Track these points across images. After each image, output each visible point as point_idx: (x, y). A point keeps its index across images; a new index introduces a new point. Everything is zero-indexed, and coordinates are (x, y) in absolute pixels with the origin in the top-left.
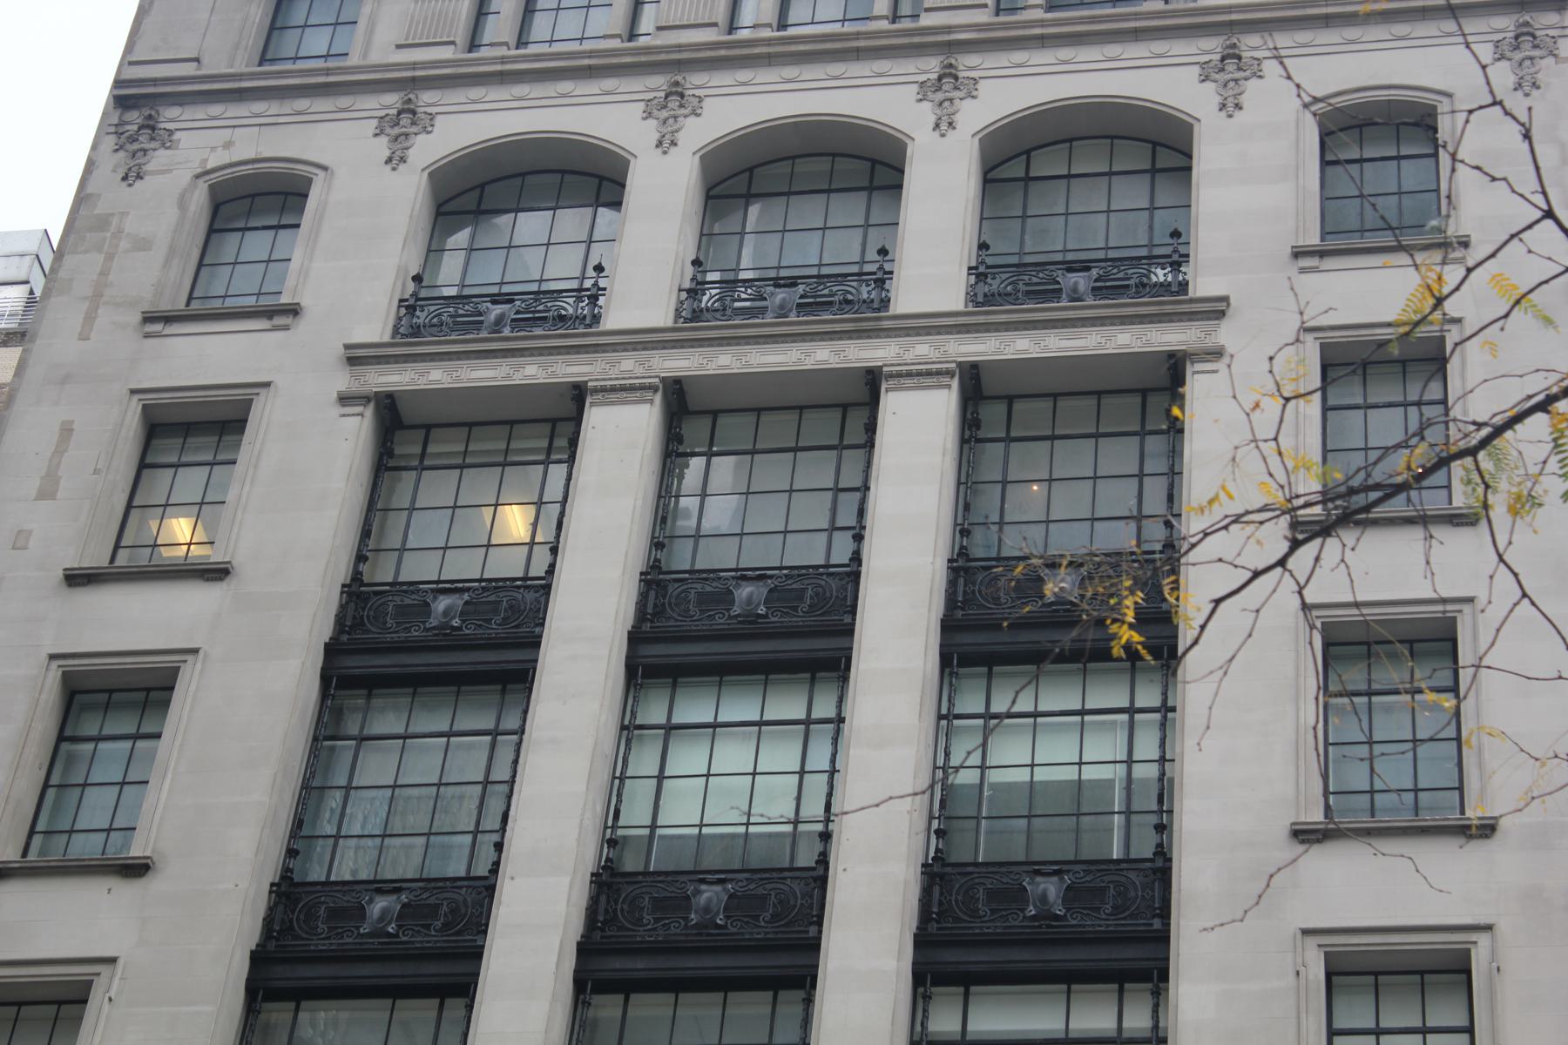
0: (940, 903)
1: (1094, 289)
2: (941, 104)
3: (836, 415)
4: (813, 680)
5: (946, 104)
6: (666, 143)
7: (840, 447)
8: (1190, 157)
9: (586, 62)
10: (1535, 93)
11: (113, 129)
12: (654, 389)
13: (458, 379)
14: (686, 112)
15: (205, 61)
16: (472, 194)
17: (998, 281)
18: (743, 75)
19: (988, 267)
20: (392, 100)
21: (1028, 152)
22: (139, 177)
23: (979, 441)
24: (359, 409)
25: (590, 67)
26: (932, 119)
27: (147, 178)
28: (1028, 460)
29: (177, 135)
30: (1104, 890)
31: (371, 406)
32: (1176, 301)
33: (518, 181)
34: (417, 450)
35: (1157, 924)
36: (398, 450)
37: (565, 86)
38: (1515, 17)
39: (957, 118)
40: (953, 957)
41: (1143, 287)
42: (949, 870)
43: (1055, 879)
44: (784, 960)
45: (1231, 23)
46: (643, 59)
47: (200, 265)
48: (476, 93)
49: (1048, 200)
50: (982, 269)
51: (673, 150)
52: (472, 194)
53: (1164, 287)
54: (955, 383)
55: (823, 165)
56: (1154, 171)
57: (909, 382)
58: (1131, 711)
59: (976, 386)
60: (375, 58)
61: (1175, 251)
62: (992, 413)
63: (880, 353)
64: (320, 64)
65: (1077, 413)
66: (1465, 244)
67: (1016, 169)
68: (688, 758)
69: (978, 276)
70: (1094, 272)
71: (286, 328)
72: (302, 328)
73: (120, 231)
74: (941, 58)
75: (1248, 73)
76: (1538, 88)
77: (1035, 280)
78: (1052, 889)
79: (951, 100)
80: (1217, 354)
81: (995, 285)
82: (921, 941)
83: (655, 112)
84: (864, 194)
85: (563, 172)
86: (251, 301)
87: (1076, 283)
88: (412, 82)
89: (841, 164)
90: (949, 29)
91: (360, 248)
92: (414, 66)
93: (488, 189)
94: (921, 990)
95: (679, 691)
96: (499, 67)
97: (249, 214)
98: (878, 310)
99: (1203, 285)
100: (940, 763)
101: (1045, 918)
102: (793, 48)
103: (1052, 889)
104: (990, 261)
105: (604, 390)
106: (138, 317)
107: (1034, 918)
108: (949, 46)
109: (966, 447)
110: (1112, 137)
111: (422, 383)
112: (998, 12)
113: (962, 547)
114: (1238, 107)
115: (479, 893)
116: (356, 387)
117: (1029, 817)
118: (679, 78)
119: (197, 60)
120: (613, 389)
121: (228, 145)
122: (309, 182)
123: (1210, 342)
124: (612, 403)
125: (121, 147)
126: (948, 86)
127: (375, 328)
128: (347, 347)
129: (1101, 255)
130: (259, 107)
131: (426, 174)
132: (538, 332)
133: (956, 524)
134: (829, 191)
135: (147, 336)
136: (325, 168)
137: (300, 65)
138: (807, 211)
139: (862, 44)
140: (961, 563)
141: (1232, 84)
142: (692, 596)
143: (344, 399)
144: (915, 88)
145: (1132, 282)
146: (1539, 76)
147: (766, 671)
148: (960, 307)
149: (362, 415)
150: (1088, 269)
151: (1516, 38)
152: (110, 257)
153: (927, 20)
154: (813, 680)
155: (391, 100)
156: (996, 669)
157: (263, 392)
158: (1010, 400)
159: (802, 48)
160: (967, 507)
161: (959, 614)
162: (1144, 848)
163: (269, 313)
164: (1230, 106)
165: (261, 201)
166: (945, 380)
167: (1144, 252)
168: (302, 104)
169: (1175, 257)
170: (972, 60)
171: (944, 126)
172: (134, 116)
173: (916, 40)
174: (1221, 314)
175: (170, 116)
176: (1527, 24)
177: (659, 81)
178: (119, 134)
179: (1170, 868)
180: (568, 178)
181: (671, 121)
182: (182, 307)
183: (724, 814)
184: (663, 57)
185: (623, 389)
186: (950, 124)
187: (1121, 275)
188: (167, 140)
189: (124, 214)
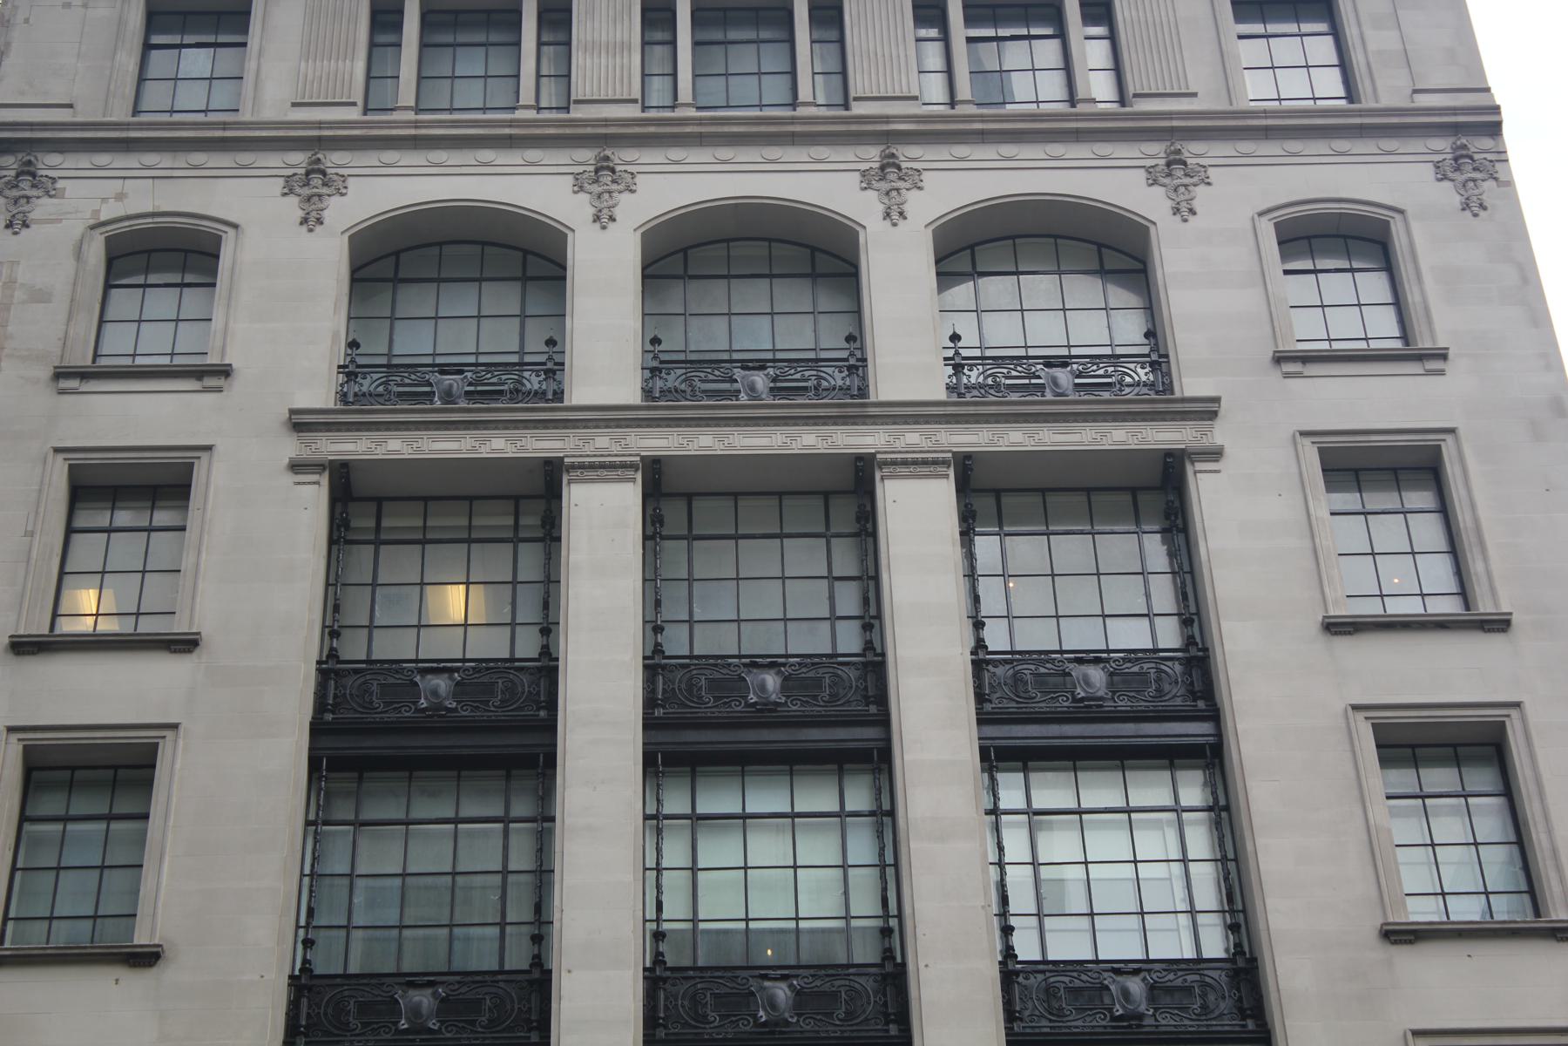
1: (772, 389)
2: (887, 194)
3: (818, 502)
4: (508, 777)
6: (603, 218)
7: (516, 540)
8: (565, 269)
9: (507, 131)
10: (1482, 213)
14: (621, 187)
15: (79, 107)
16: (391, 261)
18: (676, 154)
19: (662, 362)
20: (299, 159)
21: (972, 247)
22: (25, 225)
24: (315, 478)
25: (510, 137)
27: (33, 227)
28: (713, 559)
29: (60, 184)
31: (326, 475)
32: (1161, 400)
33: (436, 250)
34: (372, 523)
36: (353, 524)
37: (487, 155)
38: (1452, 139)
39: (906, 207)
41: (517, 393)
42: (315, 982)
43: (429, 991)
45: (1172, 130)
46: (568, 131)
47: (102, 321)
48: (390, 156)
49: (416, 300)
50: (351, 368)
51: (318, 229)
52: (391, 261)
53: (540, 395)
54: (639, 476)
57: (904, 470)
58: (841, 814)
59: (661, 485)
60: (269, 114)
61: (550, 359)
62: (674, 514)
63: (869, 440)
64: (200, 117)
65: (759, 515)
67: (963, 263)
68: (718, 850)
69: (348, 374)
70: (771, 371)
71: (219, 390)
72: (238, 387)
74: (882, 147)
75: (1195, 180)
76: (1485, 209)
77: (1014, 373)
78: (782, 992)
80: (1216, 454)
81: (366, 385)
83: (298, 190)
84: (519, 284)
85: (484, 244)
86: (166, 360)
87: (451, 386)
88: (318, 142)
90: (887, 119)
91: (285, 311)
92: (320, 125)
93: (403, 256)
95: (700, 782)
96: (413, 132)
97: (147, 270)
98: (1164, 392)
99: (1191, 385)
100: (651, 863)
101: (418, 1032)
102: (726, 129)
103: (424, 999)
104: (361, 361)
105: (582, 466)
106: (45, 373)
107: (406, 1031)
108: (886, 136)
109: (335, 548)
110: (1013, 238)
111: (380, 453)
112: (366, 111)
113: (332, 649)
114: (1192, 212)
116: (306, 454)
117: (451, 926)
118: (608, 152)
119: (70, 106)
120: (592, 466)
121: (120, 197)
122: (217, 240)
124: (592, 481)
126: (604, 180)
127: (319, 394)
128: (293, 412)
129: (472, 359)
130: (150, 159)
131: (346, 237)
132: (1106, 395)
133: (324, 627)
134: (480, 280)
135: (62, 392)
136: (235, 226)
137: (177, 117)
138: (460, 300)
139: (798, 128)
140: (330, 665)
141: (1182, 189)
142: (374, 688)
143: (296, 467)
144: (281, 181)
145: (505, 387)
146: (1484, 197)
147: (792, 762)
148: (331, 405)
149: (317, 483)
150: (763, 368)
153: (858, 109)
154: (508, 777)
156: (514, 772)
157: (204, 455)
158: (689, 497)
159: (735, 129)
160: (336, 608)
161: (329, 717)
162: (518, 958)
163: (199, 373)
164: (1184, 210)
166: (941, 469)
167: (514, 359)
168: (198, 158)
169: (550, 365)
170: (914, 151)
171: (895, 216)
173: (854, 128)
174: (1213, 415)
175: (49, 162)
176: (1464, 147)
177: (587, 155)
179: (550, 980)
180: (447, 249)
181: (606, 196)
182: (89, 363)
183: (769, 907)
184: (589, 130)
185: (603, 466)
187: (798, 376)
188: (48, 188)
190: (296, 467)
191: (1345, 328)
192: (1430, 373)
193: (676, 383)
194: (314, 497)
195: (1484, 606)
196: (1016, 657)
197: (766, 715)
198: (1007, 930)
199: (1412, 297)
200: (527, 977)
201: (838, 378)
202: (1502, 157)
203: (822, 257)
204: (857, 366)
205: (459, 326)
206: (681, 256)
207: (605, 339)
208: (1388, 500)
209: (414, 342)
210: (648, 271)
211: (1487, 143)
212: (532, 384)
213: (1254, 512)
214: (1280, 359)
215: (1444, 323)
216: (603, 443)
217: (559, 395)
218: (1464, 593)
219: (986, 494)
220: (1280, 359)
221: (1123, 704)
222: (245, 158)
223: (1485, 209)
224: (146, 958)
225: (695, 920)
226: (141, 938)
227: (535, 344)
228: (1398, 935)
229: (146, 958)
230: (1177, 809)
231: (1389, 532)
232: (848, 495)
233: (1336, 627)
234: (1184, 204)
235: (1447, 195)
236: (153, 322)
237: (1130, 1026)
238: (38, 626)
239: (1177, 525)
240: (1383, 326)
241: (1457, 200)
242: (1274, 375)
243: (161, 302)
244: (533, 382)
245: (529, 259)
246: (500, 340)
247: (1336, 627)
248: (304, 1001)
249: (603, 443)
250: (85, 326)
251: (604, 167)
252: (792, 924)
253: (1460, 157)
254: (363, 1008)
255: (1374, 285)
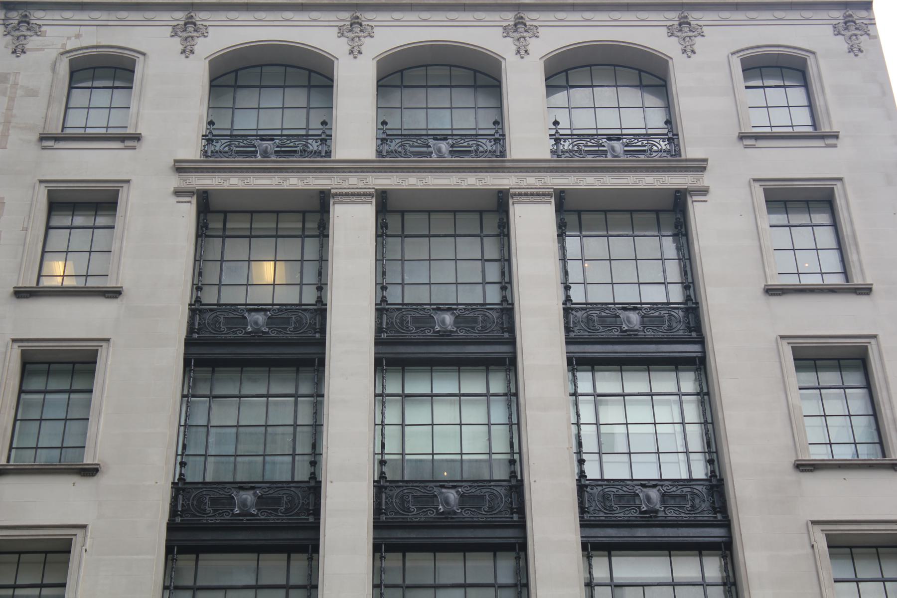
0: (386, 503)
1: (450, 151)
2: (518, 40)
3: (477, 217)
4: (298, 371)
5: (522, 40)
7: (303, 236)
8: (333, 81)
10: (860, 54)
11: (1, 22)
12: (370, 195)
13: (307, 184)
14: (365, 34)
16: (233, 75)
17: (219, 144)
19: (388, 135)
20: (181, 15)
22: (23, 52)
23: (207, 236)
26: (514, 48)
27: (28, 53)
28: (415, 249)
29: (43, 28)
30: (280, 499)
31: (195, 197)
32: (674, 160)
33: (259, 69)
34: (220, 225)
35: (311, 519)
36: (210, 226)
37: (288, 15)
39: (529, 48)
40: (399, 535)
41: (304, 152)
42: (186, 486)
43: (251, 492)
44: (301, 535)
47: (67, 108)
48: (233, 15)
49: (247, 98)
50: (210, 136)
51: (191, 56)
52: (233, 75)
53: (318, 153)
54: (374, 200)
55: (445, 71)
56: (310, 87)
58: (488, 395)
59: (386, 205)
61: (324, 132)
62: (394, 222)
63: (506, 181)
65: (442, 224)
66: (836, 137)
68: (417, 414)
69: (208, 140)
70: (450, 141)
71: (134, 148)
72: (144, 147)
73: (15, 84)
75: (695, 33)
76: (862, 52)
77: (589, 144)
78: (452, 495)
79: (524, 38)
80: (704, 191)
81: (218, 146)
82: (172, 528)
85: (286, 66)
86: (103, 131)
87: (267, 147)
89: (455, 71)
91: (172, 102)
93: (240, 73)
94: (170, 556)
95: (407, 375)
97: (93, 79)
98: (675, 155)
99: (691, 151)
100: (378, 421)
101: (245, 515)
103: (249, 497)
104: (215, 132)
105: (341, 194)
106: (37, 136)
107: (238, 515)
109: (200, 239)
110: (590, 66)
111: (226, 185)
113: (197, 297)
114: (693, 52)
115: (313, 489)
116: (183, 185)
117: (264, 456)
118: (358, 14)
120: (347, 195)
121: (78, 36)
122: (133, 62)
123: (699, 184)
125: (9, 33)
127: (192, 151)
128: (176, 161)
129: (279, 132)
130: (96, 14)
132: (642, 157)
133: (193, 284)
134: (284, 87)
135: (44, 148)
136: (144, 54)
138: (272, 98)
140: (197, 306)
141: (688, 39)
142: (222, 320)
143: (178, 193)
144: (170, 29)
145: (298, 149)
146: (861, 45)
147: (460, 365)
148: (198, 158)
150: (446, 139)
151: (846, 23)
152: (12, 99)
154: (298, 371)
155: (180, 16)
156: (301, 369)
157: (125, 185)
160: (200, 274)
161: (196, 336)
162: (303, 474)
163: (122, 138)
164: (688, 51)
165: (107, 71)
166: (547, 199)
167: (303, 132)
168: (123, 14)
169: (323, 136)
170: (534, 15)
171: (523, 52)
172: (15, 15)
174: (703, 169)
176: (851, 16)
177: (346, 15)
178: (6, 26)
180: (265, 69)
181: (357, 39)
182: (60, 131)
183: (446, 446)
185: (353, 194)
186: (526, 51)
187: (466, 144)
188: (36, 30)
189: (17, 74)
190: (178, 193)
191: (780, 119)
192: (828, 146)
193: (397, 147)
194: (188, 210)
195: (857, 280)
196: (588, 306)
197: (445, 338)
198: (581, 462)
199: (819, 102)
200: (307, 485)
201: (488, 146)
202: (872, 22)
203: (480, 76)
204: (500, 138)
205: (272, 113)
206: (399, 75)
207: (355, 121)
208: (803, 218)
209: (246, 122)
210: (380, 83)
211: (863, 14)
212: (313, 147)
213: (727, 226)
214: (742, 137)
215: (835, 118)
216: (353, 181)
217: (328, 154)
218: (845, 272)
219: (573, 214)
220: (742, 137)
221: (649, 334)
222: (150, 15)
223: (862, 52)
224: (91, 471)
225: (403, 454)
226: (88, 460)
227: (315, 124)
228: (804, 467)
229: (91, 471)
230: (679, 394)
231: (803, 237)
232: (494, 212)
233: (771, 291)
234: (689, 47)
235: (840, 44)
236: (96, 108)
237: (650, 517)
238: (30, 282)
239: (682, 231)
240: (802, 119)
241: (846, 47)
242: (739, 146)
243: (101, 97)
244: (314, 146)
245: (312, 75)
246: (295, 122)
247: (771, 291)
248: (180, 497)
249: (353, 181)
250: (58, 110)
251: (356, 22)
252: (459, 457)
253: (848, 22)
254: (214, 501)
255: (797, 95)
